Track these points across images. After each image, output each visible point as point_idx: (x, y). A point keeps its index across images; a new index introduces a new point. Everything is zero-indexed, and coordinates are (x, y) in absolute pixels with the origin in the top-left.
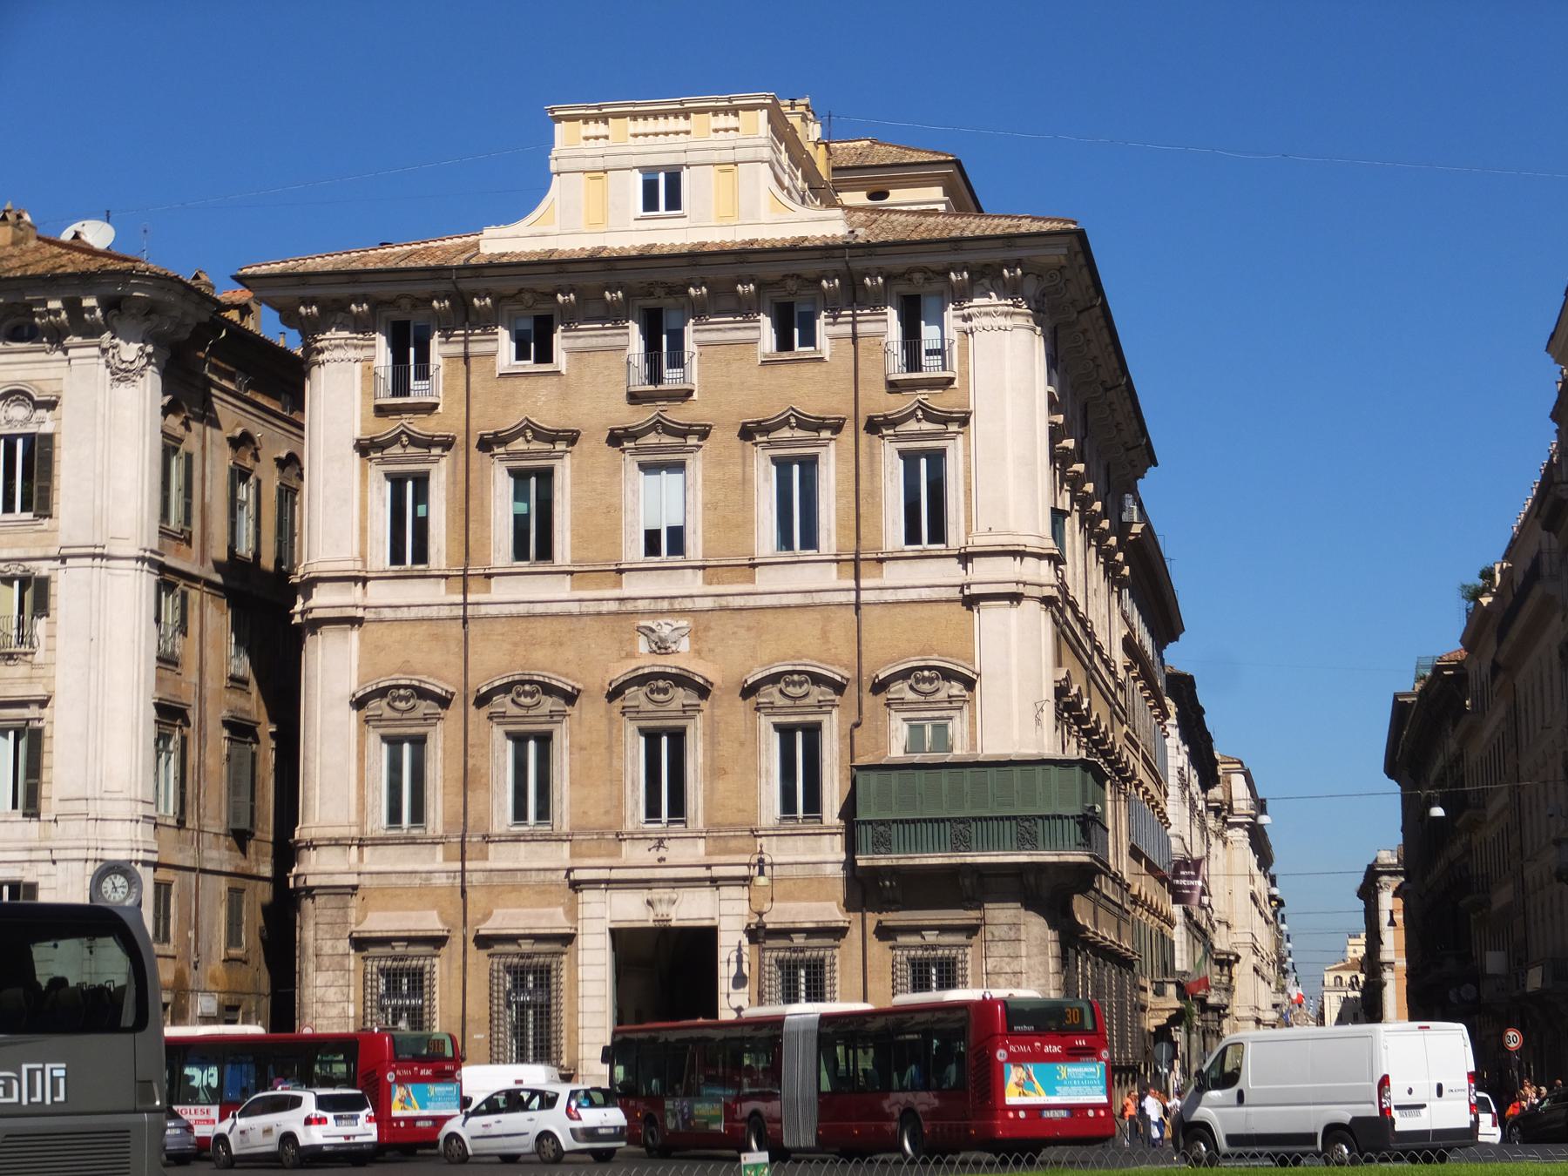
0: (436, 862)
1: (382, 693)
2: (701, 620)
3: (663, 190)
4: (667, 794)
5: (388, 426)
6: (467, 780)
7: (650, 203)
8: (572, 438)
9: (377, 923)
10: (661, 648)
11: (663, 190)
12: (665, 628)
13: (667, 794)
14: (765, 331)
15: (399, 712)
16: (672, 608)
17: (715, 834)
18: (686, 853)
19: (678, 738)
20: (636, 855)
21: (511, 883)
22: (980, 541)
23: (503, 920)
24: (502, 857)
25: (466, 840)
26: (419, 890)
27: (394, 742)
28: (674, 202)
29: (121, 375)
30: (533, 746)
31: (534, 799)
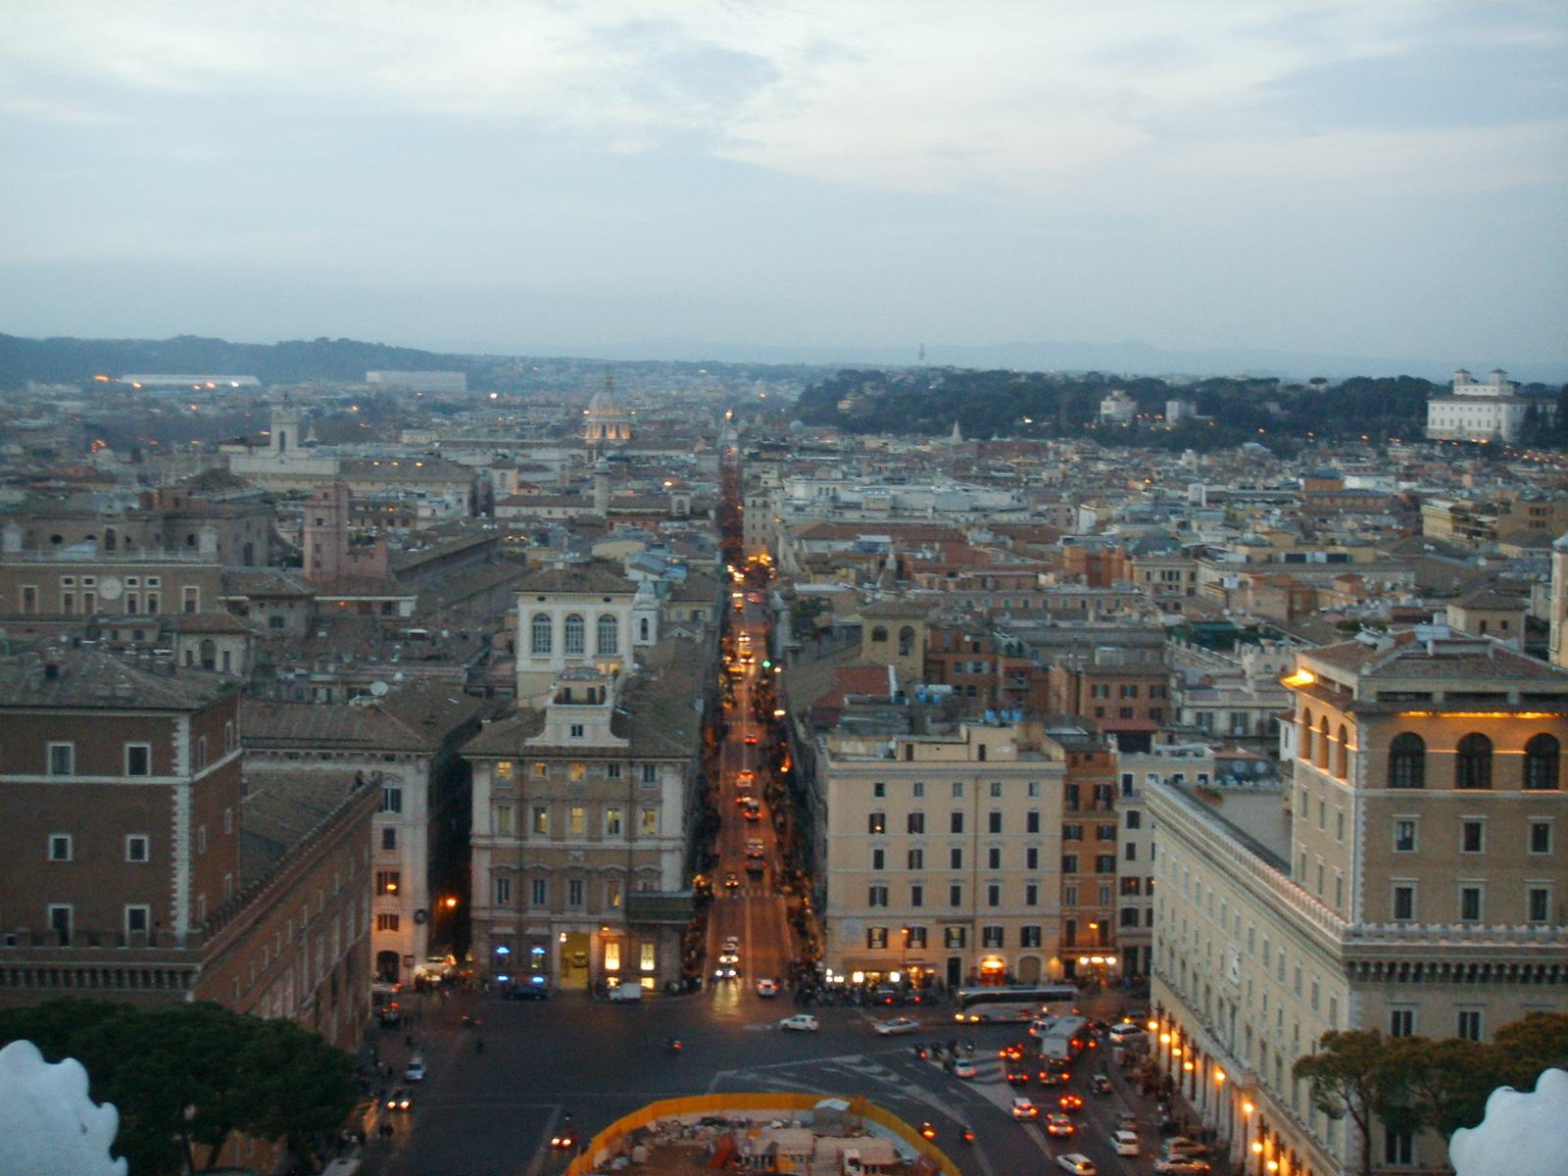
0: (512, 915)
1: (499, 868)
2: (588, 852)
3: (577, 731)
4: (576, 899)
5: (500, 795)
6: (522, 891)
7: (574, 734)
8: (553, 800)
9: (497, 930)
10: (576, 859)
11: (577, 731)
12: (578, 854)
13: (576, 899)
14: (605, 774)
15: (500, 876)
16: (579, 848)
17: (591, 913)
18: (582, 915)
19: (579, 882)
20: (568, 915)
21: (530, 922)
22: (664, 835)
23: (531, 931)
24: (532, 914)
25: (521, 908)
26: (507, 922)
27: (500, 881)
28: (581, 734)
29: (419, 772)
30: (539, 884)
31: (539, 899)
